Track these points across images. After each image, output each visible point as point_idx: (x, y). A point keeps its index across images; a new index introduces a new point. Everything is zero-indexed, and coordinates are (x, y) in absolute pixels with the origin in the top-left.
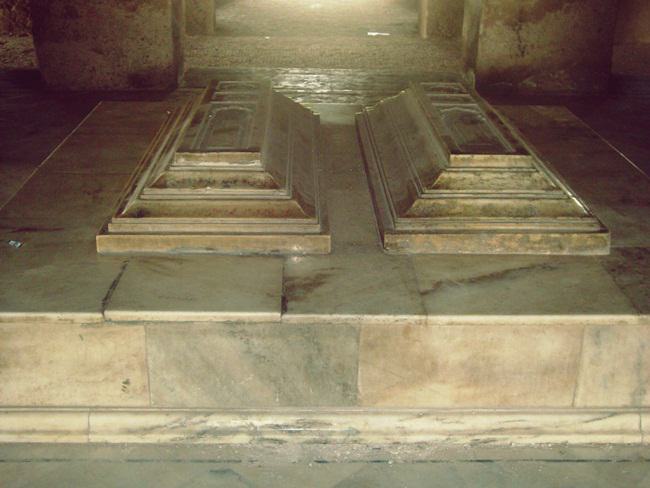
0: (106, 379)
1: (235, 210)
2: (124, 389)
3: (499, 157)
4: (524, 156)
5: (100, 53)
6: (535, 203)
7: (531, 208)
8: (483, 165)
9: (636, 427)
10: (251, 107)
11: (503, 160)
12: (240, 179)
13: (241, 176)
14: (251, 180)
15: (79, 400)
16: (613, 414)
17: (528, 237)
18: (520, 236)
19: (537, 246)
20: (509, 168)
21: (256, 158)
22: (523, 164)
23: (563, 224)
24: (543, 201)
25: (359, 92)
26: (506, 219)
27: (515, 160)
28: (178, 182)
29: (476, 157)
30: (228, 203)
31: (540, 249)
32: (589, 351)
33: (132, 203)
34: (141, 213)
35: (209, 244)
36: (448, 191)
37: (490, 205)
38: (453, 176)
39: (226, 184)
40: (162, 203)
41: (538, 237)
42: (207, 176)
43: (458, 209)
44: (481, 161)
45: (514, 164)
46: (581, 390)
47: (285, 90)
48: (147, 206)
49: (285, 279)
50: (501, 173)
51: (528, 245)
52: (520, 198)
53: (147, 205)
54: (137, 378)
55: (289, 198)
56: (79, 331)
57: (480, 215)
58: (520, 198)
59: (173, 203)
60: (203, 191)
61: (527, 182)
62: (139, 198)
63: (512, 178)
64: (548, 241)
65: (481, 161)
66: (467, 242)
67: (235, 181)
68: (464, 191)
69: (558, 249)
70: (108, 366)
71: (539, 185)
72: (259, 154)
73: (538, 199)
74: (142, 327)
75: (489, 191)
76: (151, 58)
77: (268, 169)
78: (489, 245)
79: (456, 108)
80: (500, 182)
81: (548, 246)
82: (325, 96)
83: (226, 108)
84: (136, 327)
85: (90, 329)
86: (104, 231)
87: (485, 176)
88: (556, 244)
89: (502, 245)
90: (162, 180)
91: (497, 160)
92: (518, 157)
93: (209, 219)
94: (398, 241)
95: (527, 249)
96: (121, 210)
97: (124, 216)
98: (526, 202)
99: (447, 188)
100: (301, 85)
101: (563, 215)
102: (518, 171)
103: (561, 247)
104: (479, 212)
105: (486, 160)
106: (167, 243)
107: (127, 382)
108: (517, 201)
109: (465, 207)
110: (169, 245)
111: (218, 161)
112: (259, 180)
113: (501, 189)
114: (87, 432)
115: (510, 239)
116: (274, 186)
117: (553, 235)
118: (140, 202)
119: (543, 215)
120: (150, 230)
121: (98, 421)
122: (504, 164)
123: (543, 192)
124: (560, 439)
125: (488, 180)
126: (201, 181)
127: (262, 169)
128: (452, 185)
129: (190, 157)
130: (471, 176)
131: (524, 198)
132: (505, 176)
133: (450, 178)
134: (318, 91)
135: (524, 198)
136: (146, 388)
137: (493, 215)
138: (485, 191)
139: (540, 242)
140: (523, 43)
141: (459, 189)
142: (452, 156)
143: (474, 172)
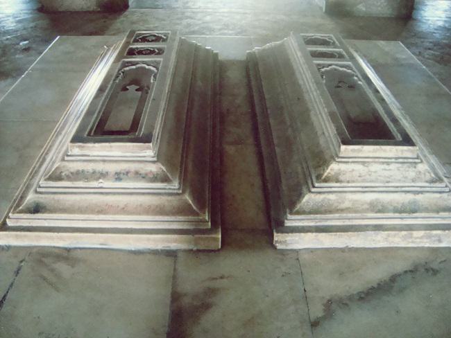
1: (126, 206)
4: (410, 147)
6: (419, 197)
7: (415, 202)
8: (371, 155)
10: (156, 65)
11: (391, 151)
12: (133, 170)
13: (133, 167)
14: (142, 172)
17: (412, 234)
18: (404, 233)
19: (418, 240)
20: (396, 158)
21: (148, 148)
22: (409, 155)
24: (427, 195)
25: (248, 11)
26: (391, 215)
27: (402, 151)
28: (72, 173)
30: (120, 198)
31: (420, 242)
33: (31, 197)
34: (36, 209)
35: (102, 241)
36: (338, 185)
37: (377, 199)
38: (343, 167)
39: (118, 176)
40: (57, 197)
41: (422, 233)
42: (100, 167)
44: (369, 152)
47: (198, 10)
48: (42, 201)
49: (176, 297)
50: (388, 164)
51: (410, 240)
53: (43, 199)
55: (181, 192)
57: (366, 211)
60: (95, 184)
61: (411, 173)
62: (36, 192)
64: (430, 237)
65: (369, 152)
66: (353, 238)
67: (127, 173)
68: (353, 185)
69: (437, 242)
71: (423, 176)
72: (151, 144)
73: (422, 192)
75: (377, 185)
77: (160, 157)
78: (374, 240)
79: (334, 66)
80: (387, 173)
81: (428, 241)
82: (226, 15)
83: (134, 67)
87: (374, 167)
88: (437, 238)
89: (386, 239)
90: (58, 172)
91: (385, 151)
92: (405, 148)
93: (102, 217)
94: (287, 239)
95: (409, 242)
96: (18, 205)
97: (21, 212)
98: (410, 197)
99: (337, 181)
100: (210, 5)
102: (402, 161)
103: (440, 241)
104: (366, 206)
105: (374, 151)
106: (61, 239)
108: (403, 195)
110: (64, 240)
111: (112, 151)
112: (151, 172)
113: (388, 182)
115: (395, 236)
116: (165, 179)
117: (434, 232)
118: (37, 195)
119: (427, 210)
120: (46, 224)
123: (427, 184)
125: (375, 172)
126: (94, 172)
127: (155, 159)
128: (341, 178)
129: (83, 147)
130: (359, 167)
131: (408, 192)
132: (393, 166)
133: (340, 170)
134: (222, 10)
135: (408, 192)
137: (379, 211)
138: (373, 185)
139: (422, 238)
141: (348, 182)
142: (343, 147)
143: (363, 163)
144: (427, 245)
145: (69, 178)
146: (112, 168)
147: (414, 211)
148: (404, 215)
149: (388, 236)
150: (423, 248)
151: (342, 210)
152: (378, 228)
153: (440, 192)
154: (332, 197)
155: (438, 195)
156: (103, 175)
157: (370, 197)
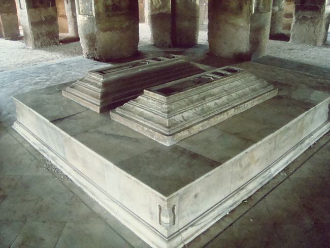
3: (157, 95)
6: (155, 116)
22: (163, 100)
23: (157, 127)
29: (150, 92)
30: (89, 90)
37: (142, 112)
45: (160, 99)
52: (153, 113)
58: (153, 113)
59: (80, 86)
63: (156, 104)
73: (157, 115)
76: (241, 49)
86: (65, 90)
91: (156, 95)
98: (153, 115)
101: (160, 124)
105: (153, 95)
109: (136, 109)
122: (158, 98)
124: (97, 200)
130: (146, 99)
132: (155, 102)
143: (148, 98)
144: (150, 137)
146: (92, 81)
147: (150, 120)
148: (146, 120)
150: (146, 137)
151: (130, 111)
152: (137, 122)
153: (163, 117)
154: (131, 106)
155: (161, 117)
156: (89, 82)
157: (142, 110)
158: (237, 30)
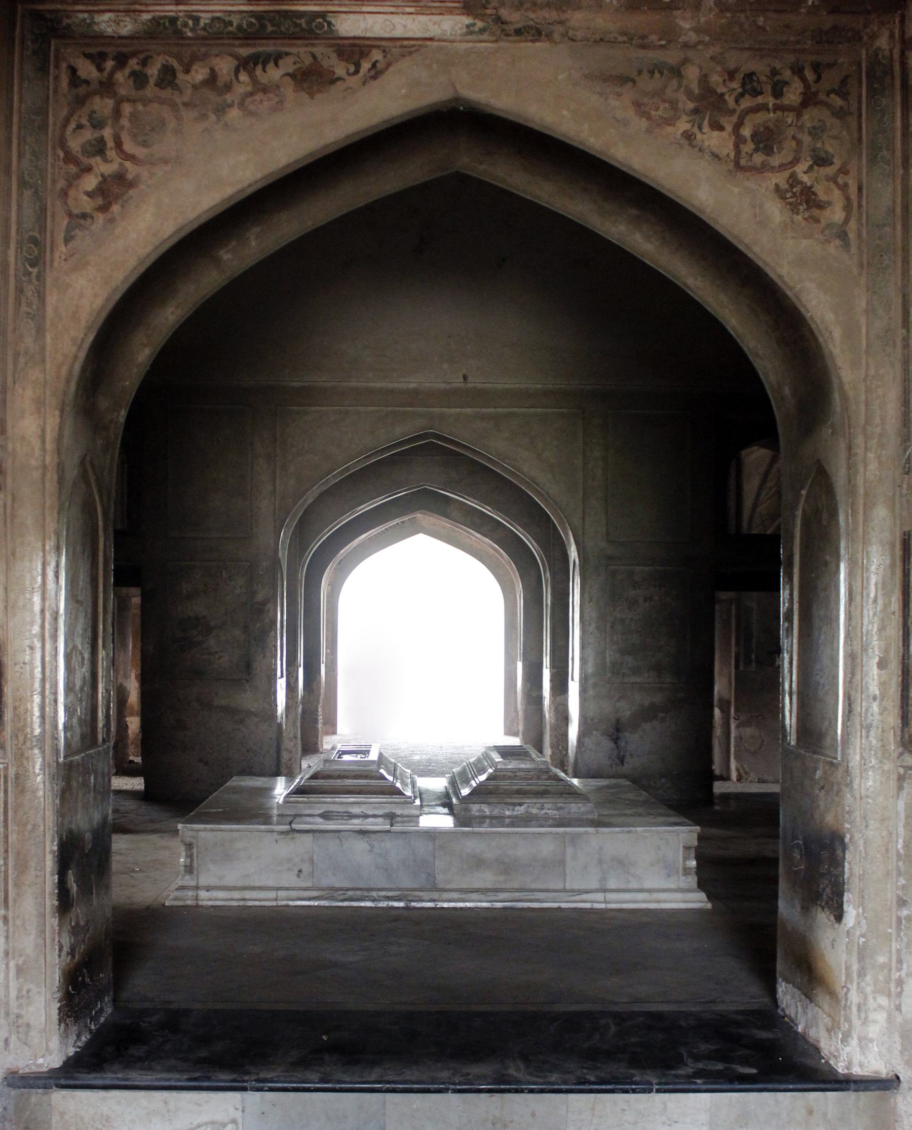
0: (289, 869)
2: (298, 876)
5: (206, 763)
9: (602, 899)
15: (270, 883)
16: (587, 892)
32: (569, 851)
39: (356, 777)
43: (500, 791)
46: (568, 879)
54: (306, 868)
56: (278, 837)
70: (289, 860)
74: (311, 835)
84: (306, 835)
85: (283, 836)
107: (300, 871)
114: (276, 900)
115: (533, 807)
121: (282, 894)
136: (312, 874)
140: (622, 753)
145: (323, 778)
149: (528, 807)
158: (242, 722)
